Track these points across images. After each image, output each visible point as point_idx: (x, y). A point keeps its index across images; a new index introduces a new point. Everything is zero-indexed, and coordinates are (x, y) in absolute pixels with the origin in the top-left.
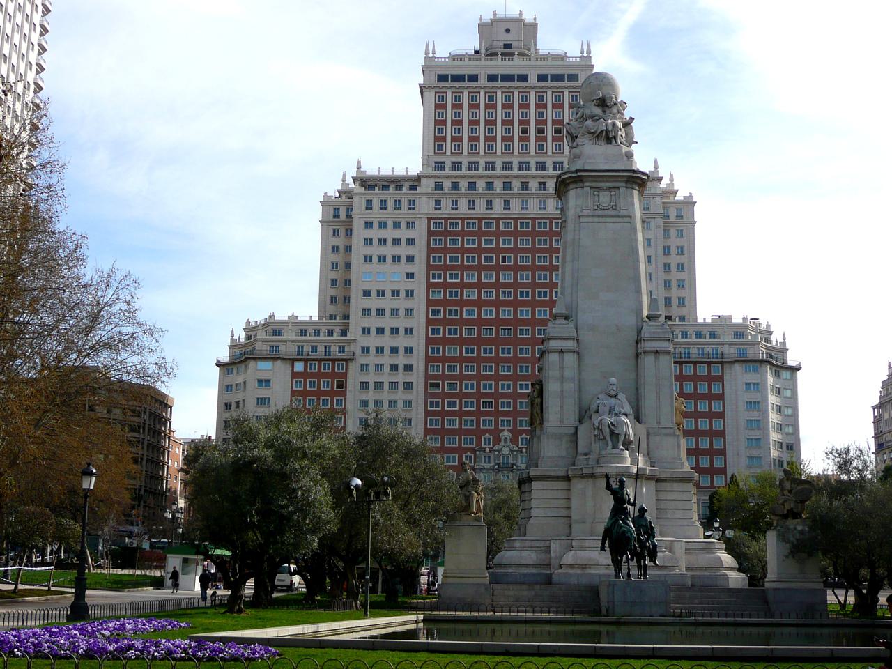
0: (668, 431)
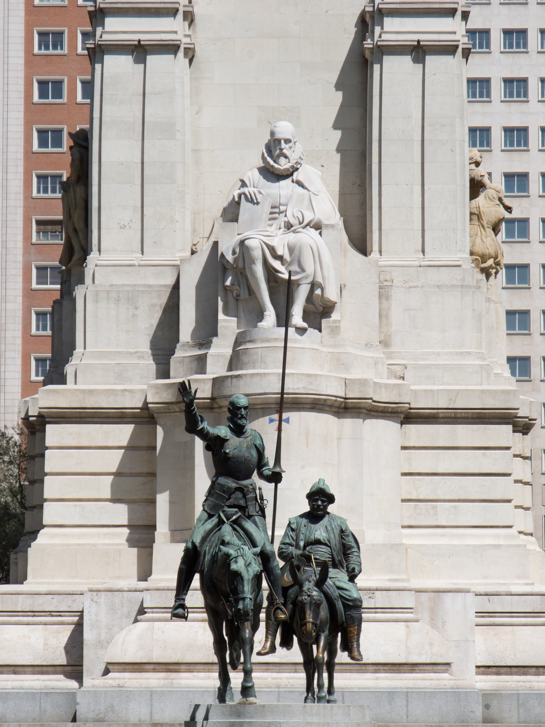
0: (444, 276)
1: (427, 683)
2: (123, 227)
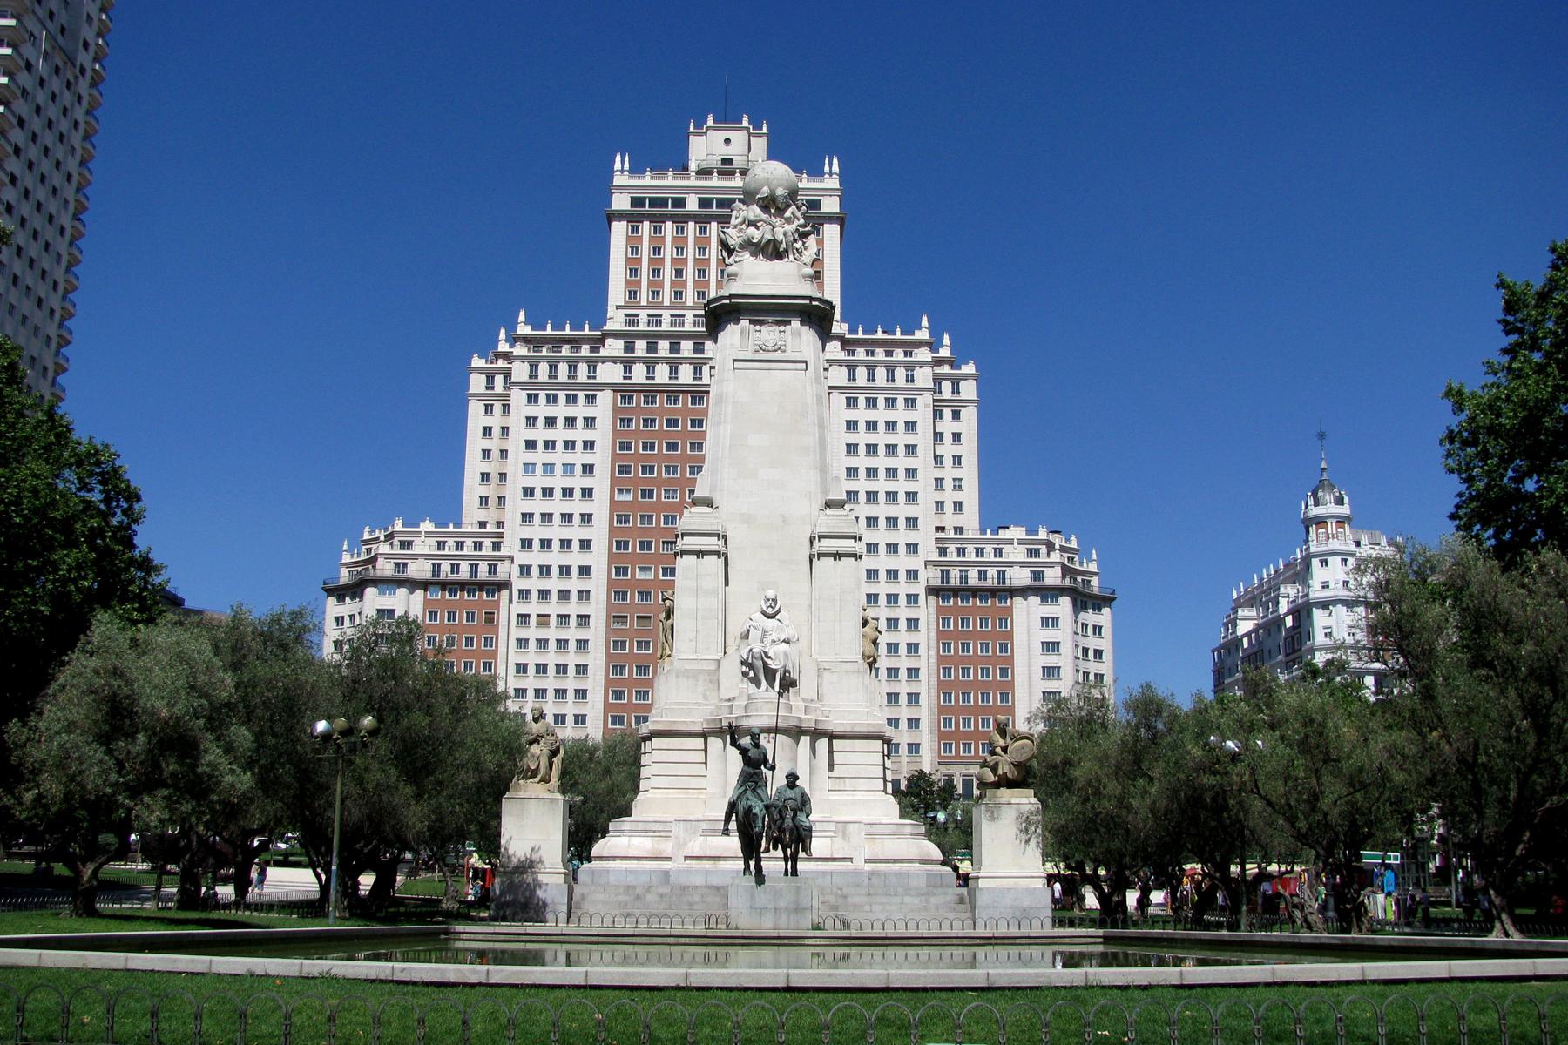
0: (849, 667)
1: (841, 868)
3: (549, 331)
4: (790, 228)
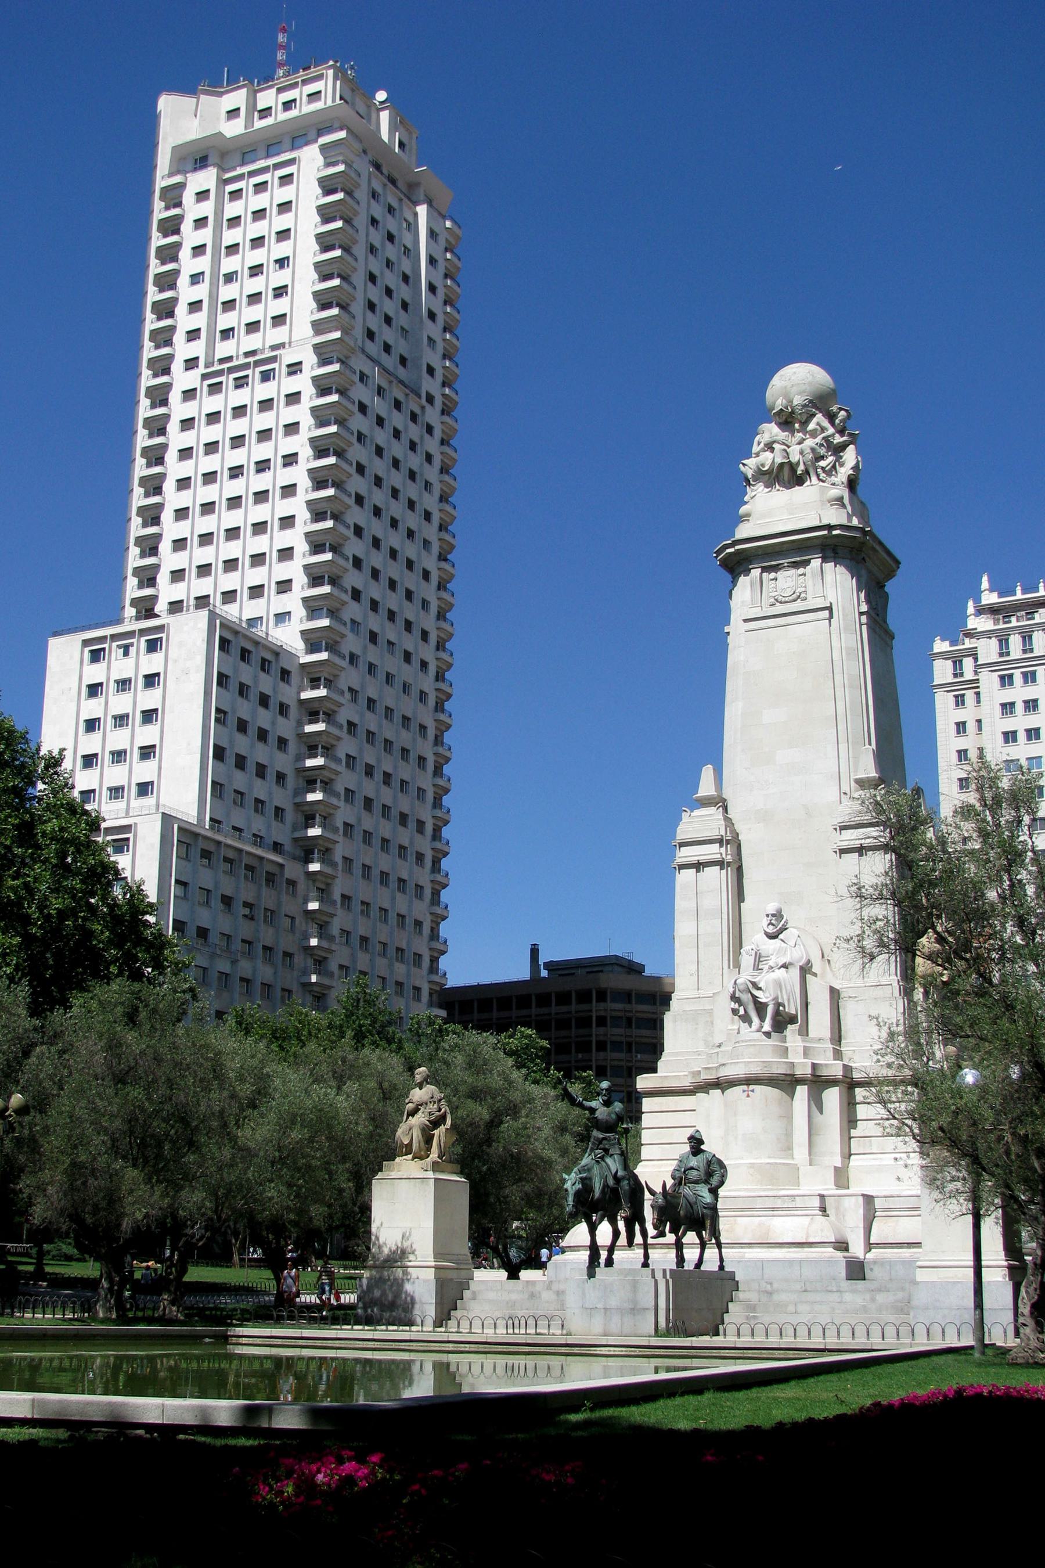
0: (879, 992)
1: (814, 1255)
2: (691, 975)
3: (1019, 595)
4: (810, 442)
